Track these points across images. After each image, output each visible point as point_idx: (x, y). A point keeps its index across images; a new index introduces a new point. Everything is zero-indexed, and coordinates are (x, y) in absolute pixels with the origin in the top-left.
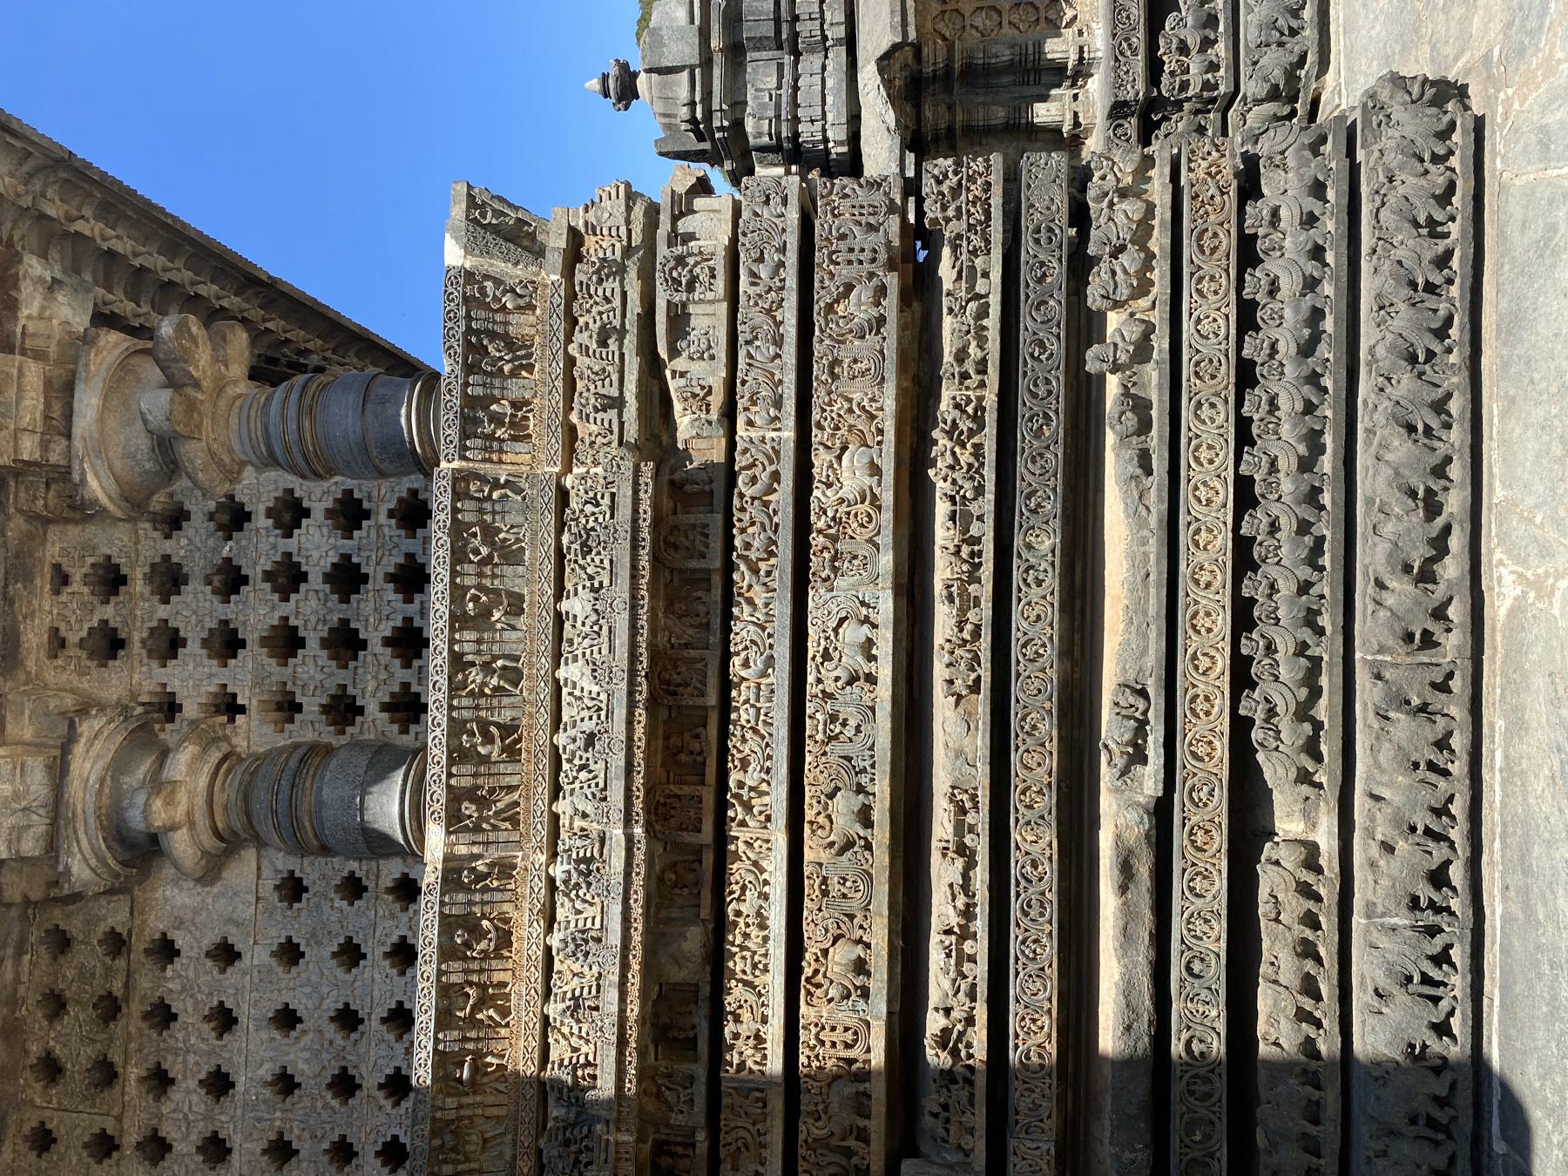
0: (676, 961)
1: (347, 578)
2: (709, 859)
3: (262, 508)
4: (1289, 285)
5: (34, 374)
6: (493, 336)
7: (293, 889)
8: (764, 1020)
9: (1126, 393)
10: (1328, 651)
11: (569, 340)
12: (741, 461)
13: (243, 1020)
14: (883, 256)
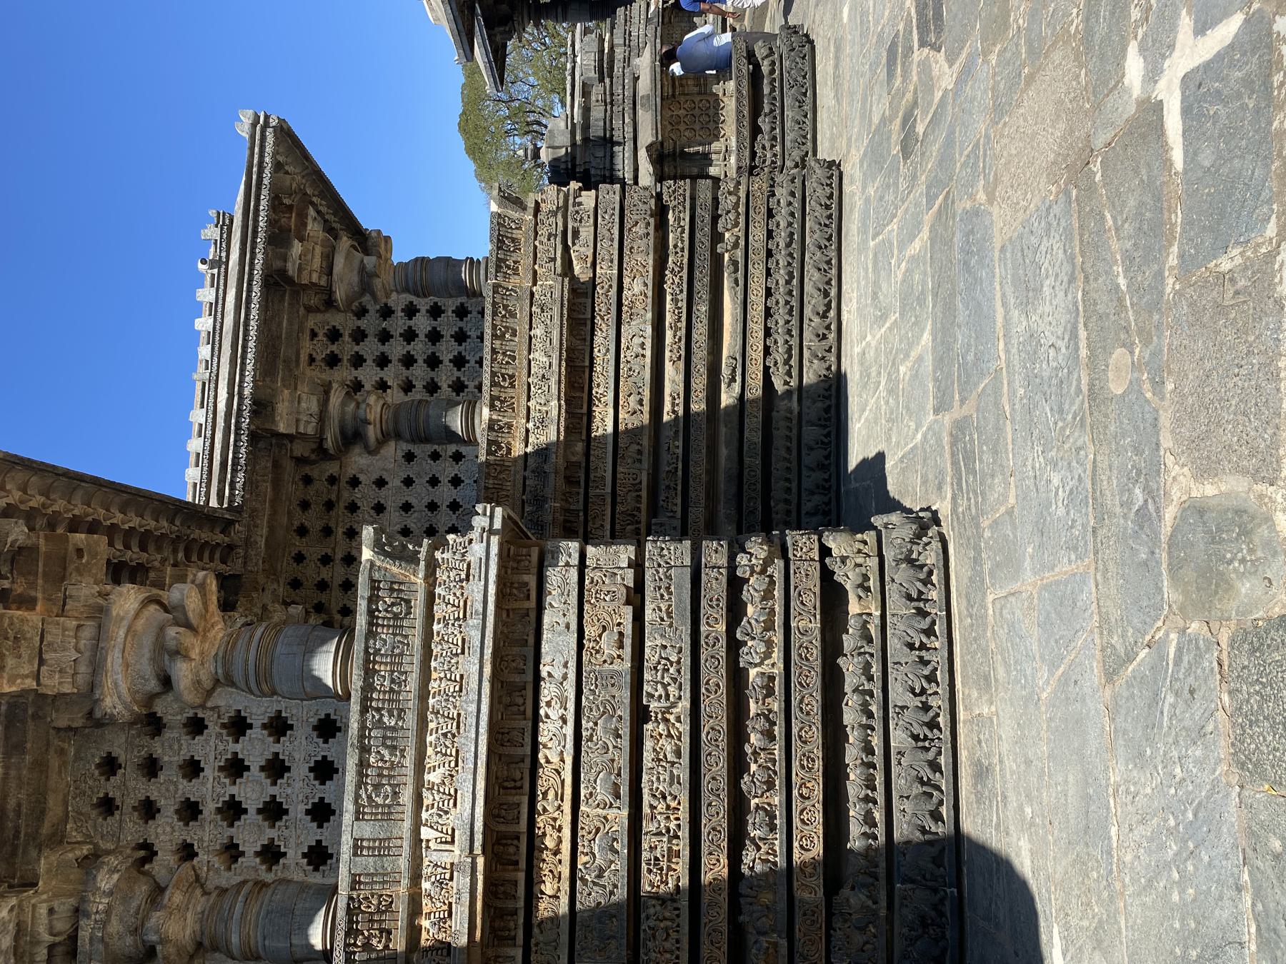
0: (573, 454)
1: (434, 336)
2: (585, 419)
3: (400, 309)
4: (783, 224)
5: (318, 250)
6: (507, 237)
7: (410, 457)
8: (605, 471)
9: (730, 259)
10: (794, 342)
11: (535, 239)
12: (598, 281)
13: (388, 508)
14: (649, 212)
